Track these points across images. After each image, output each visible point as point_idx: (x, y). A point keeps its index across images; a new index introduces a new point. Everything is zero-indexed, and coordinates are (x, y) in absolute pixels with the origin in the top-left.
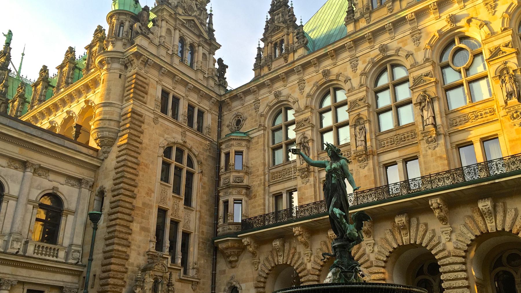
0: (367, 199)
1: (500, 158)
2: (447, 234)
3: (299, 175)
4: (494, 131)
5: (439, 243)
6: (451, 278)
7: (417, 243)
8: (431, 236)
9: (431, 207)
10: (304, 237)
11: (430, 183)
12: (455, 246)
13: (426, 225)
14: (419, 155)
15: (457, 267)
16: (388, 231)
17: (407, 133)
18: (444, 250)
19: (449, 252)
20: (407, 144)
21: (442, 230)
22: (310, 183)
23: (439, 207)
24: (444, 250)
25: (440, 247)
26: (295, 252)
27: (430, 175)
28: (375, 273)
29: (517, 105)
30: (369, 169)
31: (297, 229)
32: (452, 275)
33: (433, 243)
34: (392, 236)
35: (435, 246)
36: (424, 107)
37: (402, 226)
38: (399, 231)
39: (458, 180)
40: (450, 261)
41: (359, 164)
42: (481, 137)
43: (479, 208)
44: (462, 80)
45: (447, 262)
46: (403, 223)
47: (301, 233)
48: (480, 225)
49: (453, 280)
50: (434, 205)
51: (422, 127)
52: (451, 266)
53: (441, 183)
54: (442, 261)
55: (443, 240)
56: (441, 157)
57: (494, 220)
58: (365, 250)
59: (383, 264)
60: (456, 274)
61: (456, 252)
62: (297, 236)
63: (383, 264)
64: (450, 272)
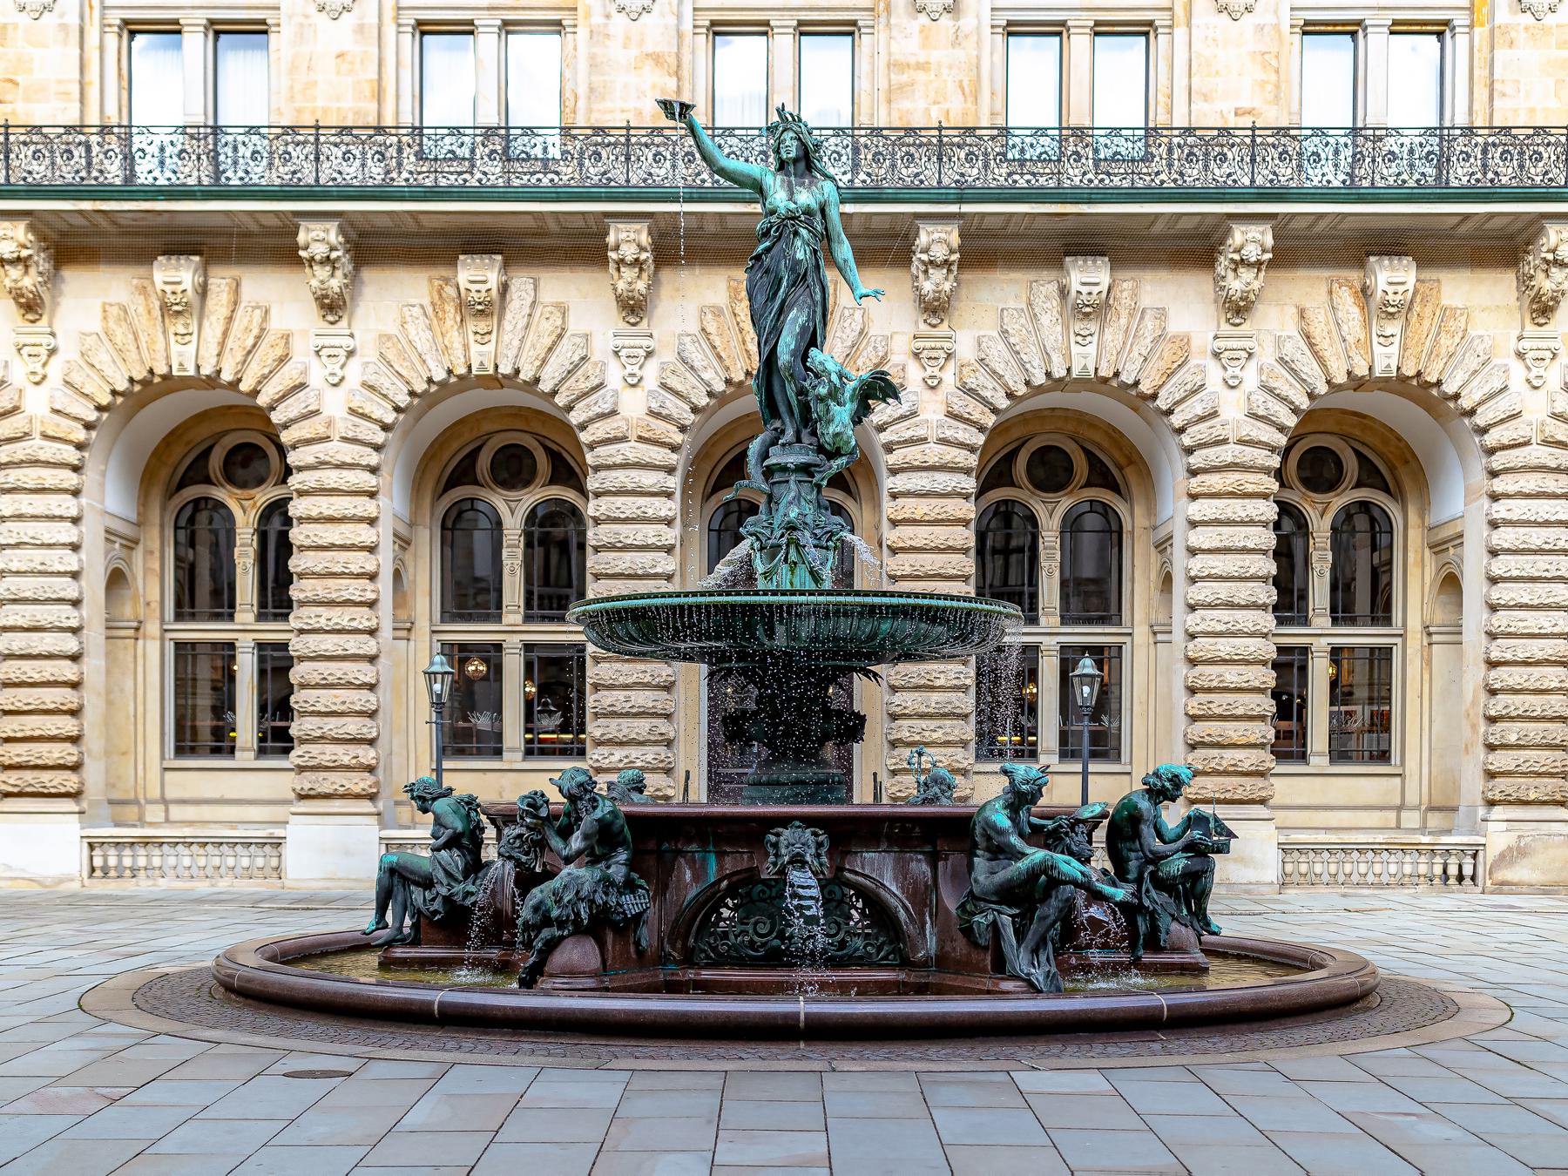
1: (873, 129)
2: (634, 361)
4: (847, 9)
6: (622, 516)
8: (576, 358)
9: (610, 254)
11: (623, 159)
12: (655, 406)
13: (564, 311)
14: (571, 22)
15: (649, 479)
16: (417, 311)
18: (613, 413)
21: (620, 342)
22: (62, 15)
23: (637, 260)
24: (613, 413)
25: (601, 403)
27: (628, 128)
28: (341, 466)
30: (360, 29)
32: (629, 505)
33: (579, 383)
35: (585, 395)
37: (480, 303)
38: (458, 319)
40: (630, 456)
45: (619, 460)
49: (627, 520)
50: (624, 247)
52: (628, 472)
54: (600, 450)
56: (657, 59)
58: (304, 372)
59: (380, 437)
61: (653, 427)
63: (380, 437)
64: (622, 492)
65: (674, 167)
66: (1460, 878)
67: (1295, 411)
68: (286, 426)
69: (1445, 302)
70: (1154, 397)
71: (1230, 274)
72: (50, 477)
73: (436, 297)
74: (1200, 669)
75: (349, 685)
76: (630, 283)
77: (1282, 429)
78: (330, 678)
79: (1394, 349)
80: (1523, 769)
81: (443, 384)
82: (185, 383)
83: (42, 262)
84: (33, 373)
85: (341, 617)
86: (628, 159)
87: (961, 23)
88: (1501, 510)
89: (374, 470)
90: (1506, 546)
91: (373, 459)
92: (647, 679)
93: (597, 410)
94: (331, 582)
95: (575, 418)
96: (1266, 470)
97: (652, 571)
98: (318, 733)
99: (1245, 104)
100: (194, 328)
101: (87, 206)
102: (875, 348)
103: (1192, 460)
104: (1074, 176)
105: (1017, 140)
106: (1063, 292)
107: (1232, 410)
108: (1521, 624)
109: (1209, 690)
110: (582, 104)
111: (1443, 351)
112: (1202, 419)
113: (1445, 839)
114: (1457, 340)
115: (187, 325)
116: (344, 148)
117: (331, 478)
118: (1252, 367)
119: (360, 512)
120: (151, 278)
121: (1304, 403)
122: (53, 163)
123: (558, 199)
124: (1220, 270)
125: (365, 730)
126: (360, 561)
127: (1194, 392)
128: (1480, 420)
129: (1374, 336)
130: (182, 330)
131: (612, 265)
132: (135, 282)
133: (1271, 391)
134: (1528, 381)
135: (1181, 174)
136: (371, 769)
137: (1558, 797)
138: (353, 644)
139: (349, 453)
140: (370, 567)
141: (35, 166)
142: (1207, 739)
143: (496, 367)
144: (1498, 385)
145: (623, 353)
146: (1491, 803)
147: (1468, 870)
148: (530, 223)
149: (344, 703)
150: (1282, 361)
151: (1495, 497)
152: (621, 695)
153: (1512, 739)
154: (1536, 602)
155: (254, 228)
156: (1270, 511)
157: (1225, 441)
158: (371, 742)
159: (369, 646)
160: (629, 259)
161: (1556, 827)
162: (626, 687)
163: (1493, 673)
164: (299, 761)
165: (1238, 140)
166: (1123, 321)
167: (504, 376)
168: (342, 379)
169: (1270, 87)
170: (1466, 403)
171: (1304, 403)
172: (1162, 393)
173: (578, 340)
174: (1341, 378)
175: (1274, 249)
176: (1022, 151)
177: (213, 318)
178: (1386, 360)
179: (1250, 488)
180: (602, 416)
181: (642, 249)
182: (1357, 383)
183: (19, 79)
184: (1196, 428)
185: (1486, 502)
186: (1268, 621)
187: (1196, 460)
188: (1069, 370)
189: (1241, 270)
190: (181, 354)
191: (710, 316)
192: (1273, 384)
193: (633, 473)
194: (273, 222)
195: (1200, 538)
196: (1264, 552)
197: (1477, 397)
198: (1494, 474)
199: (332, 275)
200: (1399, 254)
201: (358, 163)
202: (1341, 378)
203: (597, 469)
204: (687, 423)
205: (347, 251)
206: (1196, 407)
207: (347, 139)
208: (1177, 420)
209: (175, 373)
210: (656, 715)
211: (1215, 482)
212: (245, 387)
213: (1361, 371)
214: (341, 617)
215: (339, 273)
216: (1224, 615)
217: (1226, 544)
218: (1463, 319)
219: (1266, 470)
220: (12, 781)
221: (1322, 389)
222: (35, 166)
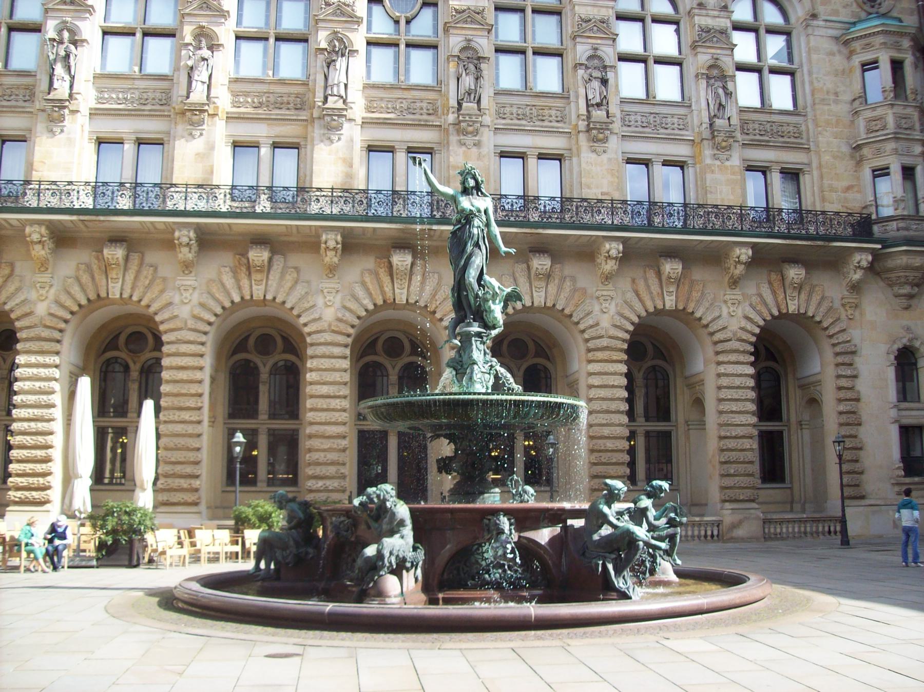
0: (207, 202)
3: (43, 111)
5: (314, 306)
7: (277, 300)
8: (303, 293)
9: (323, 246)
10: (46, 247)
12: (340, 315)
15: (337, 351)
16: (227, 269)
17: (289, 95)
19: (330, 325)
20: (286, 117)
22: (69, 134)
24: (320, 318)
26: (11, 275)
29: (475, 115)
31: (37, 230)
32: (326, 363)
34: (233, 280)
35: (307, 310)
36: (334, 61)
38: (247, 273)
39: (376, 210)
41: (189, 127)
42: (410, 145)
43: (390, 263)
44: (398, 37)
45: (322, 340)
46: (263, 261)
47: (44, 239)
48: (387, 289)
51: (322, 95)
53: (348, 208)
54: (314, 336)
55: (320, 301)
57: (406, 284)
60: (333, 360)
62: (32, 242)
64: (323, 356)
65: (353, 206)
66: (712, 536)
67: (633, 323)
68: (162, 322)
69: (694, 278)
70: (571, 316)
71: (604, 263)
72: (47, 346)
73: (237, 263)
74: (595, 441)
75: (189, 449)
76: (331, 259)
77: (627, 331)
78: (179, 446)
79: (674, 298)
80: (737, 485)
81: (238, 304)
82: (113, 302)
83: (50, 244)
84: (42, 295)
85: (186, 416)
86: (332, 202)
87: (481, 150)
88: (722, 369)
89: (203, 344)
90: (725, 385)
91: (203, 338)
92: (335, 446)
93: (312, 317)
94: (181, 399)
95: (302, 320)
96: (621, 350)
97: (338, 394)
98: (172, 472)
99: (605, 190)
100: (121, 276)
101: (74, 218)
102: (444, 291)
103: (589, 345)
104: (534, 217)
105: (510, 200)
106: (529, 268)
107: (605, 322)
108: (734, 420)
109: (600, 451)
110: (308, 178)
111: (694, 299)
112: (592, 327)
113: (706, 519)
114: (699, 294)
115: (117, 274)
116: (199, 194)
117: (184, 348)
118: (613, 304)
119: (196, 364)
120: (102, 252)
121: (636, 320)
122: (61, 198)
123: (300, 219)
124: (599, 261)
125: (195, 471)
126: (194, 388)
127: (588, 314)
128: (711, 330)
129: (665, 293)
130: (115, 276)
131: (322, 251)
132: (94, 253)
133: (622, 315)
134: (729, 313)
135: (582, 218)
136: (197, 490)
137: (752, 498)
138: (190, 429)
139: (192, 336)
140: (200, 391)
141: (52, 200)
142: (600, 474)
143: (265, 296)
144: (717, 314)
145: (325, 291)
146: (725, 501)
147: (715, 533)
148: (284, 229)
149: (185, 457)
150: (626, 302)
151: (719, 363)
152: (322, 454)
153: (732, 471)
154: (738, 410)
155: (152, 229)
156: (623, 368)
157: (602, 337)
158: (197, 477)
159: (197, 429)
160: (332, 247)
161: (752, 511)
162: (324, 450)
163: (722, 443)
164: (161, 486)
165: (605, 205)
166: (557, 281)
167: (269, 301)
168: (190, 301)
169: (615, 184)
170: (704, 322)
171: (636, 320)
172: (574, 314)
173: (304, 284)
174: (651, 310)
175: (623, 253)
176: (512, 205)
177: (130, 271)
178: (670, 302)
179: (615, 358)
180: (315, 320)
181: (337, 243)
182: (659, 312)
183: (46, 161)
184: (590, 330)
185: (713, 366)
186: (625, 419)
187: (591, 345)
188: (533, 303)
189: (608, 261)
190: (113, 287)
191: (367, 275)
192: (622, 312)
193: (329, 347)
194: (162, 227)
195: (595, 381)
196: (621, 387)
197: (709, 319)
198: (717, 353)
199: (190, 252)
200: (675, 257)
201: (205, 201)
202: (651, 310)
203: (312, 345)
204: (355, 324)
205: (197, 241)
206: (590, 321)
207: (200, 190)
208: (582, 326)
209: (110, 296)
210: (338, 464)
211: (600, 355)
212: (143, 303)
213: (660, 306)
214: (186, 416)
215: (193, 251)
216: (606, 416)
217: (605, 383)
218: (702, 285)
219: (621, 350)
220: (19, 496)
221: (644, 314)
222: (52, 200)
